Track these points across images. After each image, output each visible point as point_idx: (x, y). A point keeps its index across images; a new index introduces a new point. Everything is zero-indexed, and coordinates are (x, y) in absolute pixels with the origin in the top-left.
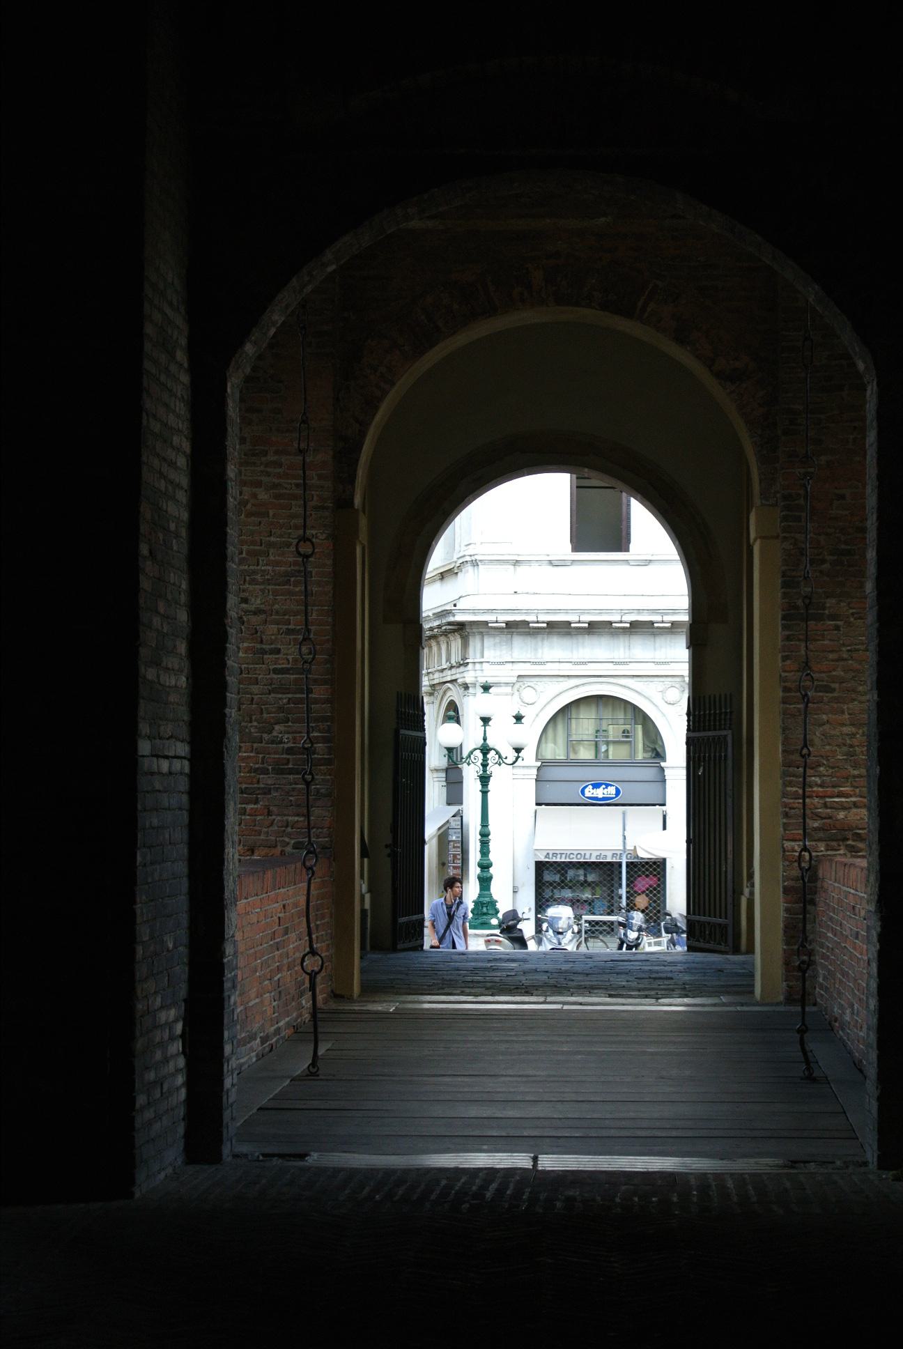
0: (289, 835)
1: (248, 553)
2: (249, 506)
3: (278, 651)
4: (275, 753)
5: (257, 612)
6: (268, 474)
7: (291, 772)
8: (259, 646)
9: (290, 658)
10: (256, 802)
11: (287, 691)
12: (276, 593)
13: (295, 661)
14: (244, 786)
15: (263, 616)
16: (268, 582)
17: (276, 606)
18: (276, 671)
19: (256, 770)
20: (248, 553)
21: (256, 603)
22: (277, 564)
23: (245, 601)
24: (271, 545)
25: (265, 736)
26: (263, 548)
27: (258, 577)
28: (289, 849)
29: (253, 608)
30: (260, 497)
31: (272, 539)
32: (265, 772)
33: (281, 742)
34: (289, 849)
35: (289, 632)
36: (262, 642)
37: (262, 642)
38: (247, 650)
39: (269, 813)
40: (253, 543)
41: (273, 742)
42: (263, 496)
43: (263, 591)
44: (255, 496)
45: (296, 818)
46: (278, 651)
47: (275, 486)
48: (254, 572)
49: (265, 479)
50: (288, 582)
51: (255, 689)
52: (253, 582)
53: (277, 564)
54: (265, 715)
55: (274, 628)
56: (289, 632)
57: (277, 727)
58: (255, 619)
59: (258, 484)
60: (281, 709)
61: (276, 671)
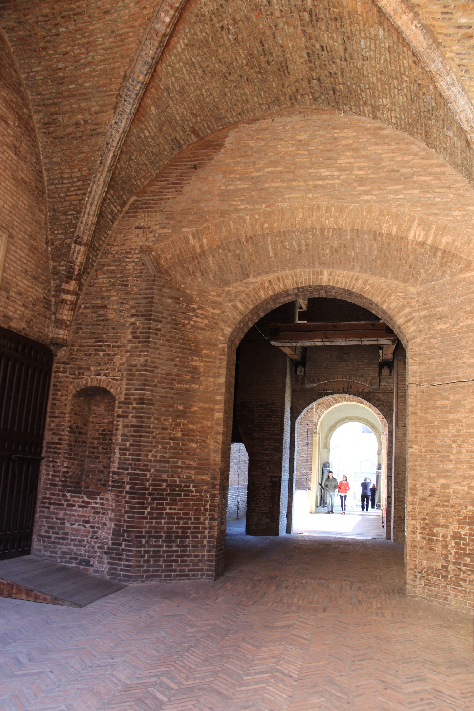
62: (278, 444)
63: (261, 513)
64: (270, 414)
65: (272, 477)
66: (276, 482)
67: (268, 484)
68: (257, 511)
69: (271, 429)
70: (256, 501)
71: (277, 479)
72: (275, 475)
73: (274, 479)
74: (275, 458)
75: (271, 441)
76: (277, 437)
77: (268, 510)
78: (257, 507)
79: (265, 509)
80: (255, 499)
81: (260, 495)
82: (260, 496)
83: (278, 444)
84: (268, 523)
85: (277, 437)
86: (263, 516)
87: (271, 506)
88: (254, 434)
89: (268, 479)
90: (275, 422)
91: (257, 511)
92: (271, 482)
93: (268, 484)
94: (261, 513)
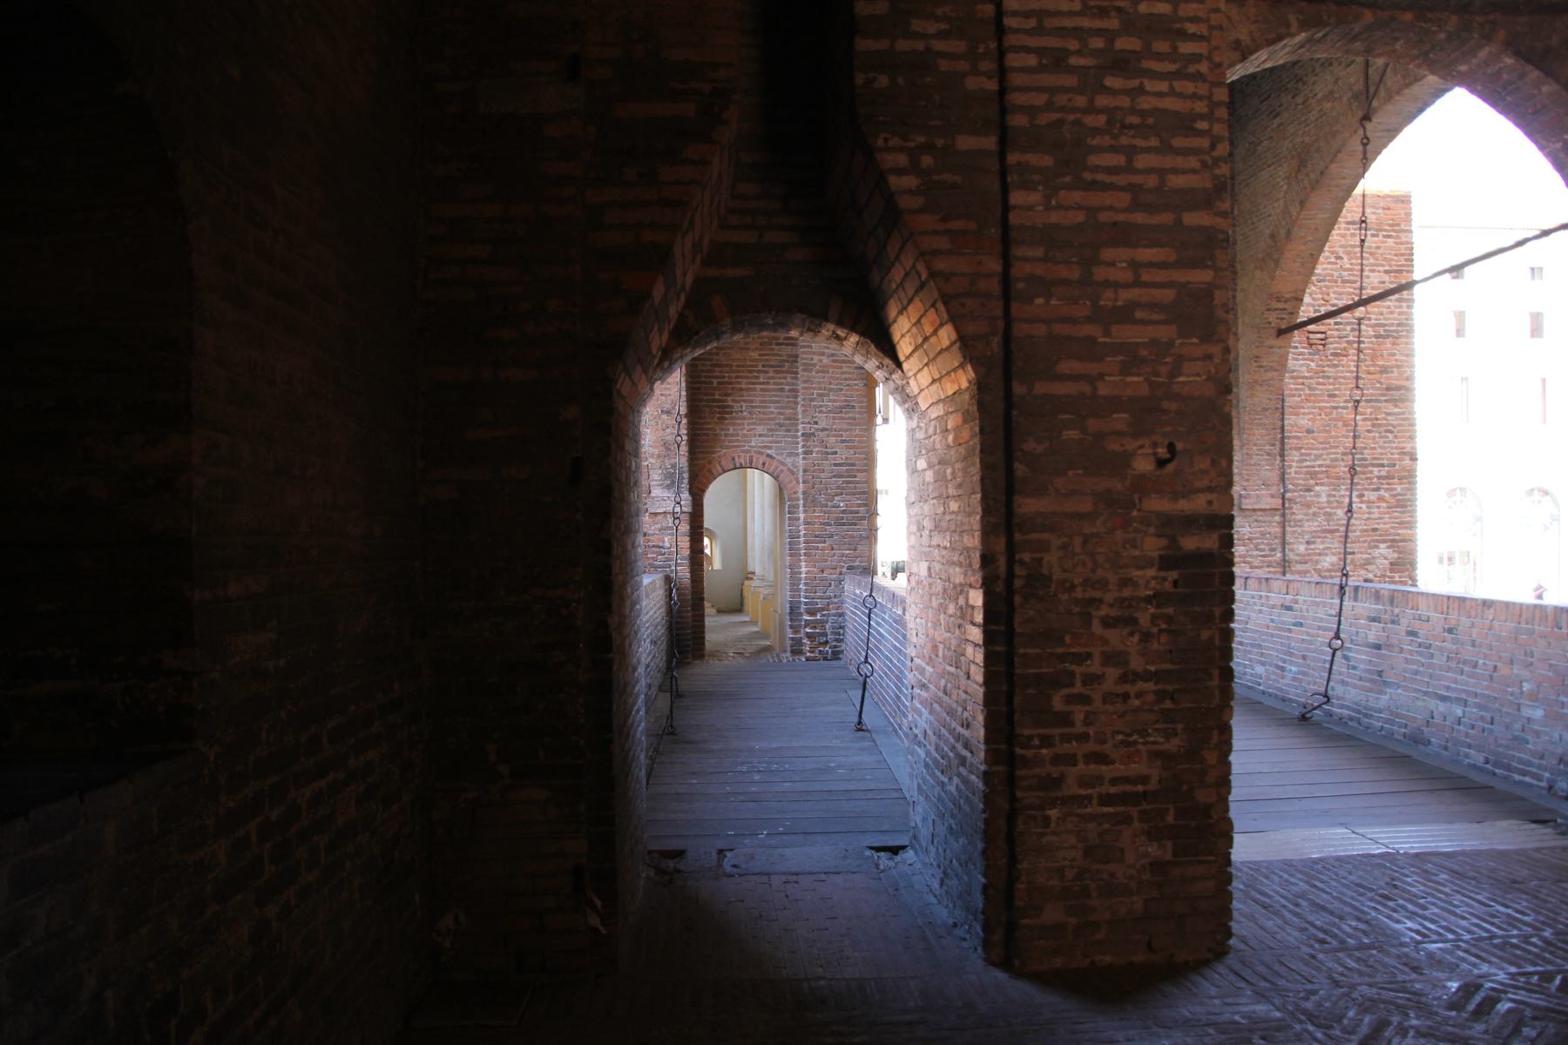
0: (844, 562)
1: (818, 394)
2: (817, 367)
3: (836, 453)
4: (836, 513)
5: (823, 430)
6: (828, 348)
7: (844, 524)
8: (824, 450)
9: (843, 457)
10: (825, 542)
11: (842, 476)
12: (834, 418)
13: (846, 458)
14: (817, 533)
15: (827, 432)
16: (830, 412)
17: (835, 427)
18: (835, 465)
19: (824, 524)
20: (818, 394)
21: (822, 425)
22: (835, 401)
23: (816, 423)
24: (830, 390)
25: (830, 504)
26: (826, 392)
27: (824, 409)
28: (844, 570)
29: (820, 427)
30: (824, 361)
31: (832, 387)
32: (829, 524)
33: (839, 507)
34: (844, 570)
35: (843, 441)
36: (826, 447)
37: (826, 447)
38: (817, 453)
39: (833, 549)
40: (820, 389)
41: (834, 507)
42: (825, 361)
43: (826, 417)
44: (821, 361)
45: (848, 552)
46: (836, 453)
47: (833, 355)
48: (821, 406)
49: (826, 351)
50: (841, 412)
51: (822, 475)
52: (820, 412)
53: (835, 401)
54: (829, 491)
55: (833, 439)
56: (843, 441)
57: (836, 498)
58: (821, 434)
59: (823, 354)
60: (838, 488)
61: (835, 465)
62: (1202, 276)
63: (1106, 800)
64: (1122, 44)
65: (1172, 525)
66: (1202, 558)
67: (1148, 579)
68: (1071, 788)
69: (1142, 162)
70: (1065, 719)
71: (1210, 542)
72: (1196, 504)
73: (1190, 543)
74: (1192, 379)
75: (1145, 254)
76: (1192, 219)
77: (1155, 773)
78: (1071, 760)
79: (1136, 768)
80: (1058, 703)
81: (1094, 666)
82: (1090, 679)
83: (1202, 276)
84: (1158, 866)
85: (1192, 219)
86: (1127, 820)
87: (1174, 745)
88: (1016, 198)
89: (1153, 546)
90: (1170, 104)
91: (1071, 788)
92: (1166, 563)
93: (1148, 579)
94: (1106, 800)
